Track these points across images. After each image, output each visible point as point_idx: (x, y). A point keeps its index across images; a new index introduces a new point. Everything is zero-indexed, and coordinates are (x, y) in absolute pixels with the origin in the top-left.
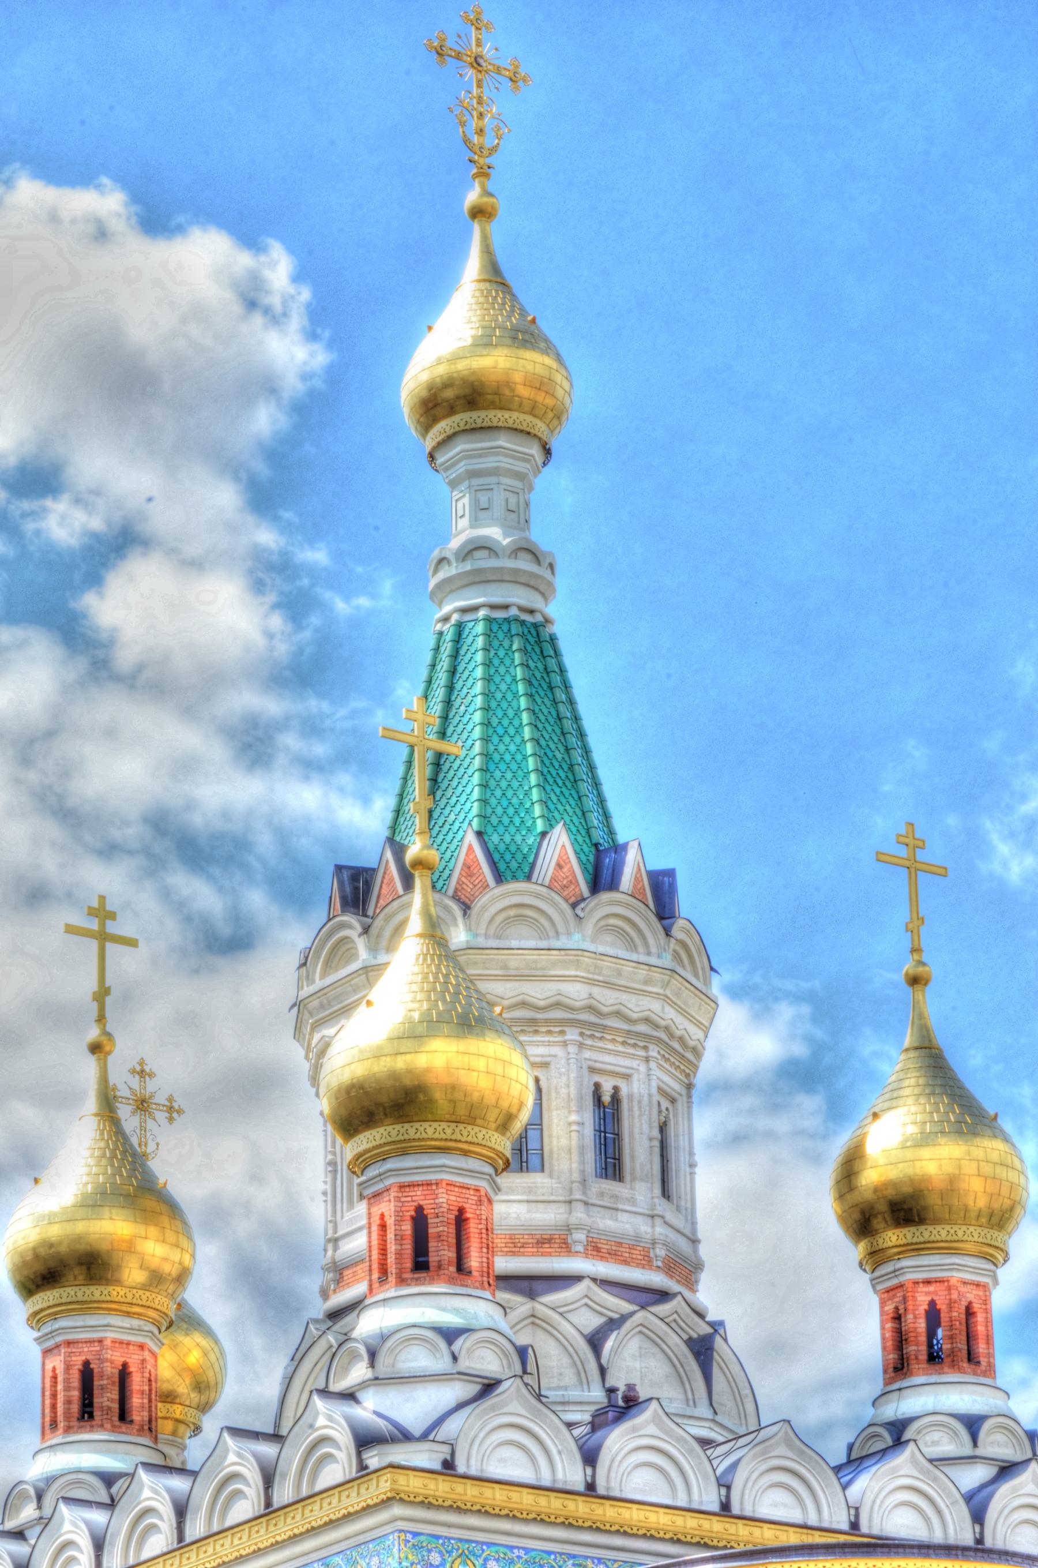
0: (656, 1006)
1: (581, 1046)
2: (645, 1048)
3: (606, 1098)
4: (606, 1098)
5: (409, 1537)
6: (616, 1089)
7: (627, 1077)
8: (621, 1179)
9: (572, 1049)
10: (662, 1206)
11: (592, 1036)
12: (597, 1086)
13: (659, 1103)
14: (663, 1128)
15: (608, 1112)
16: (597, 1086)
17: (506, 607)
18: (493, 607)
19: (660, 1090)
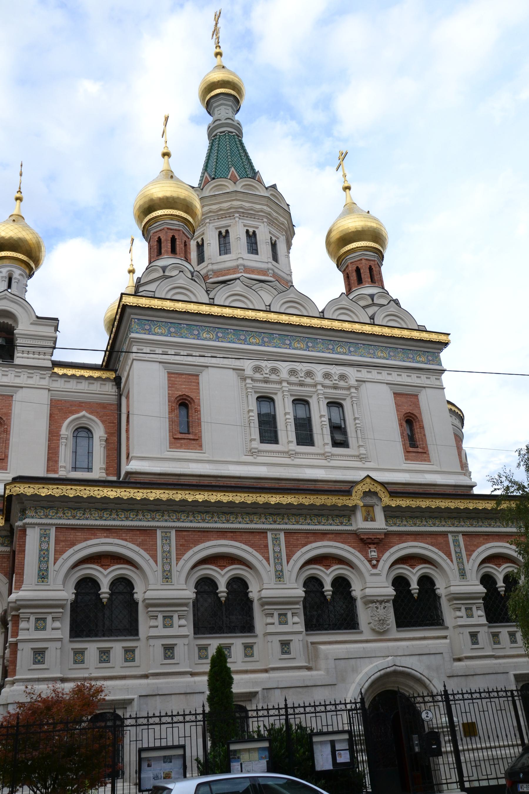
0: (265, 208)
1: (239, 218)
2: (262, 219)
3: (251, 233)
4: (251, 233)
5: (136, 320)
6: (254, 232)
7: (257, 228)
8: (257, 253)
9: (237, 219)
10: (274, 263)
11: (243, 216)
12: (247, 232)
13: (271, 238)
14: (274, 246)
15: (252, 238)
16: (247, 232)
17: (224, 132)
18: (221, 133)
19: (270, 232)
